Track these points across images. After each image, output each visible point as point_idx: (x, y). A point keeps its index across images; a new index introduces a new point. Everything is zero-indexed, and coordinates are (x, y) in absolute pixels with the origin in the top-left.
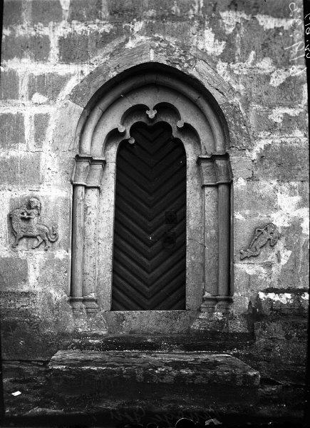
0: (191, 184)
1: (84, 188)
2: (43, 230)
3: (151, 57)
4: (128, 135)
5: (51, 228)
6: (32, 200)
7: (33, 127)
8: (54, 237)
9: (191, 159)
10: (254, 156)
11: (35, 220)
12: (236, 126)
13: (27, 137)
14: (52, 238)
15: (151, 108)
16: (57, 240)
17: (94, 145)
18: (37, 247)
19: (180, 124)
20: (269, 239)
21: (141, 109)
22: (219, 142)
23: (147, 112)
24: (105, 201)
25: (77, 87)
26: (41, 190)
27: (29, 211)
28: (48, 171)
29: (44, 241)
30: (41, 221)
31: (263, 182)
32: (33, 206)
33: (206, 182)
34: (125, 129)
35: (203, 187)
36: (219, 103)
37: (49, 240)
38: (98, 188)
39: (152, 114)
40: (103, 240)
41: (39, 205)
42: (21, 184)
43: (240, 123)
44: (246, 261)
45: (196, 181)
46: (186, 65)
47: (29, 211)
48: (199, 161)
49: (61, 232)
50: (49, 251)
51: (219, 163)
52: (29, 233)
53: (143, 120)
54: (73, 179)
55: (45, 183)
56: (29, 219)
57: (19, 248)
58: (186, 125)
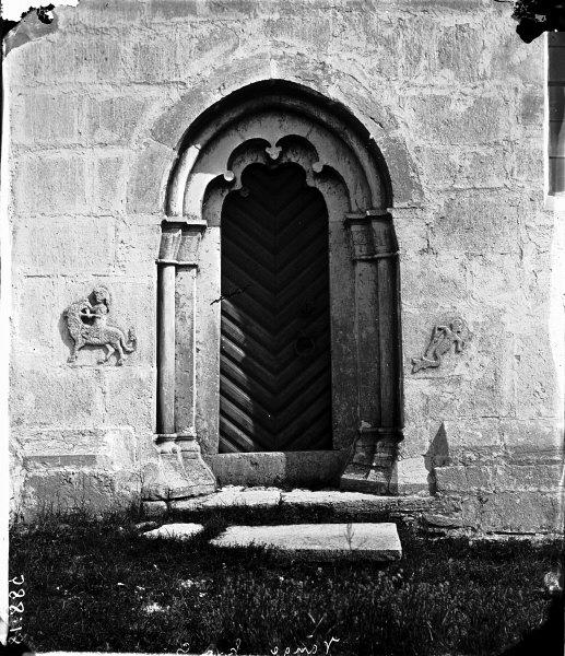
0: (336, 260)
3: (273, 72)
5: (126, 332)
6: (98, 289)
9: (335, 215)
10: (430, 216)
11: (102, 322)
17: (190, 197)
19: (318, 168)
21: (259, 145)
23: (267, 150)
25: (161, 121)
28: (120, 245)
29: (117, 352)
31: (443, 256)
32: (99, 298)
35: (354, 262)
38: (195, 266)
41: (108, 298)
44: (422, 374)
46: (325, 83)
48: (347, 223)
51: (378, 227)
53: (261, 160)
58: (325, 167)
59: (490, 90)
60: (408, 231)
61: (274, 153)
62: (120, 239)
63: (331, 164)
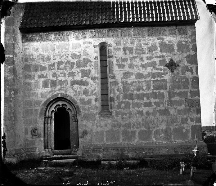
9: (70, 115)
10: (82, 116)
11: (36, 132)
19: (67, 108)
21: (59, 105)
31: (84, 121)
51: (75, 117)
59: (90, 97)
60: (79, 118)
63: (69, 108)
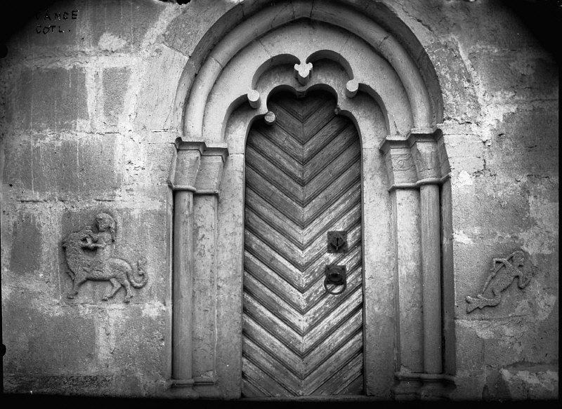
1: (191, 196)
2: (121, 268)
4: (264, 109)
5: (134, 264)
6: (101, 216)
7: (101, 92)
8: (140, 279)
10: (487, 134)
11: (106, 251)
12: (453, 82)
13: (90, 109)
14: (137, 282)
15: (303, 60)
16: (145, 284)
18: (111, 297)
19: (352, 86)
20: (517, 277)
21: (285, 64)
22: (422, 112)
24: (228, 216)
26: (117, 198)
27: (96, 236)
28: (128, 166)
30: (116, 251)
32: (102, 226)
33: (398, 182)
34: (260, 96)
35: (392, 191)
36: (423, 45)
37: (132, 285)
38: (216, 195)
39: (304, 69)
40: (225, 281)
41: (113, 226)
42: (82, 189)
43: (461, 77)
44: (476, 316)
45: (378, 180)
47: (96, 236)
49: (151, 271)
50: (133, 305)
51: (424, 148)
52: (96, 274)
53: (288, 81)
54: (172, 180)
55: (124, 188)
56: (95, 250)
57: (80, 300)
58: (361, 85)
61: (304, 69)
62: (127, 159)
